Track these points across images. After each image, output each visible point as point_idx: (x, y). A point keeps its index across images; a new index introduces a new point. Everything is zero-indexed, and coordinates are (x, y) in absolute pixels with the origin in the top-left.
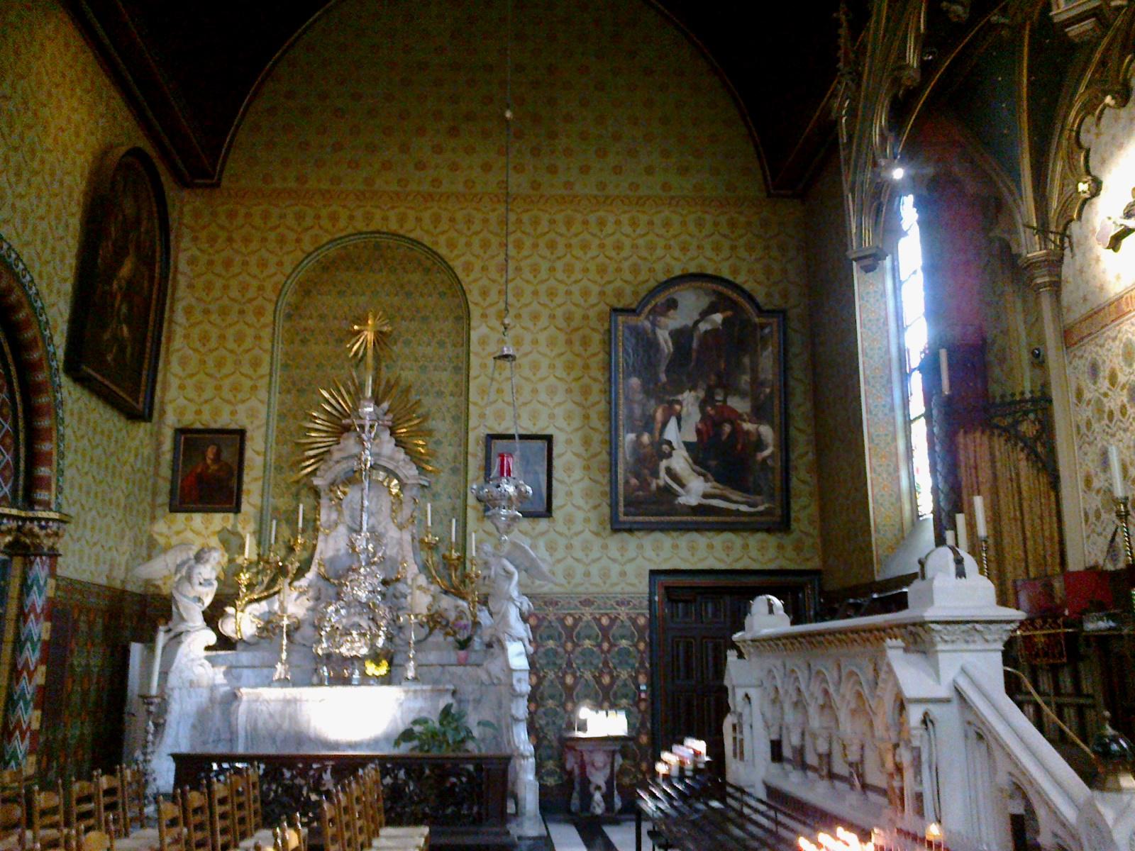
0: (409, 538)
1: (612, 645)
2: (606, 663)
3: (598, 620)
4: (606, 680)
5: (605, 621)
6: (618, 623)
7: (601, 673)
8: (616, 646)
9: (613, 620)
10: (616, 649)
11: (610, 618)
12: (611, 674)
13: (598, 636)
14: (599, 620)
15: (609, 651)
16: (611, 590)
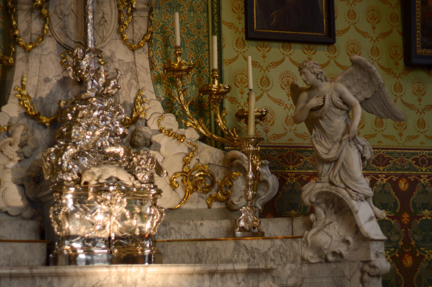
0: (147, 64)
1: (413, 217)
2: (407, 241)
3: (395, 185)
4: (409, 261)
5: (403, 185)
6: (419, 188)
7: (402, 254)
8: (418, 218)
9: (413, 184)
10: (418, 222)
11: (409, 181)
12: (412, 254)
13: (395, 204)
14: (397, 182)
15: (409, 225)
16: (409, 144)
